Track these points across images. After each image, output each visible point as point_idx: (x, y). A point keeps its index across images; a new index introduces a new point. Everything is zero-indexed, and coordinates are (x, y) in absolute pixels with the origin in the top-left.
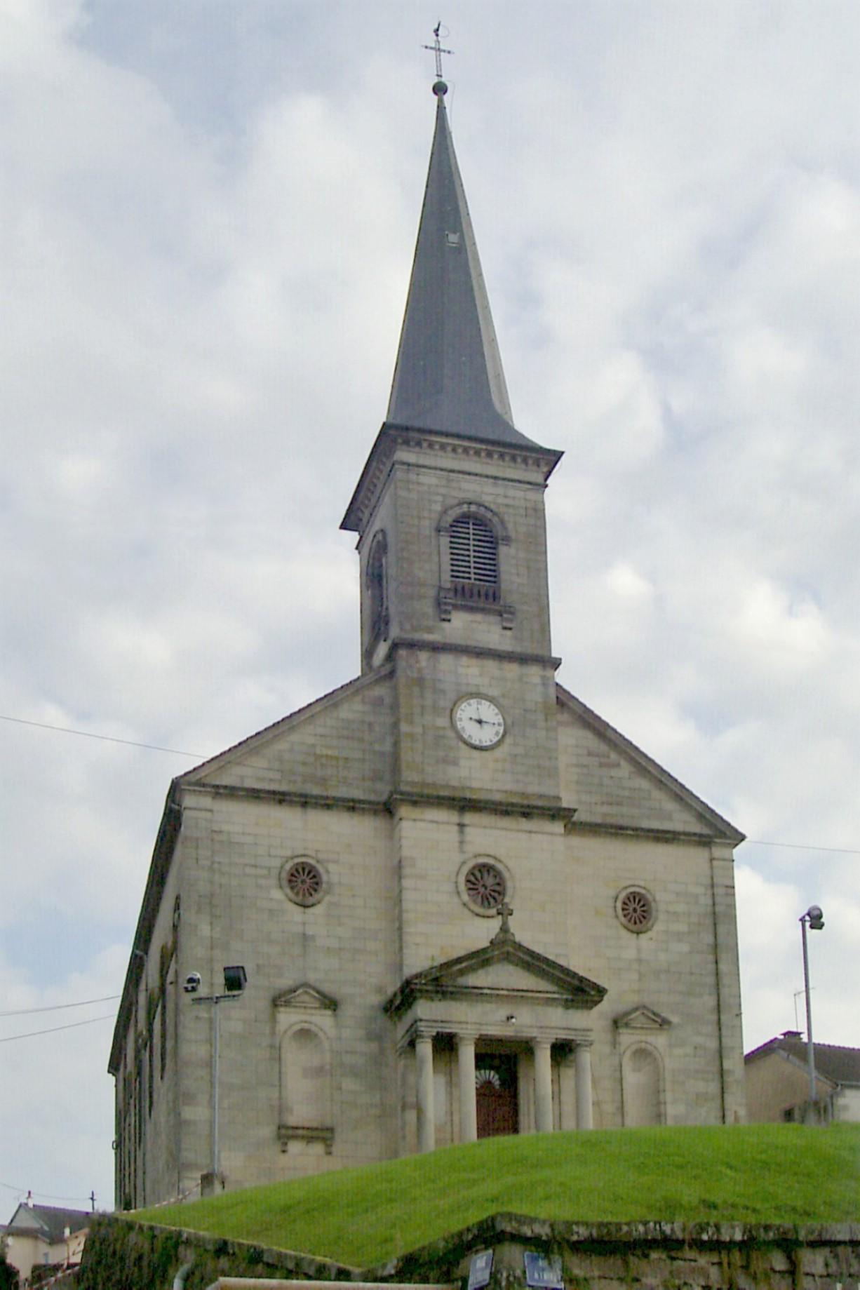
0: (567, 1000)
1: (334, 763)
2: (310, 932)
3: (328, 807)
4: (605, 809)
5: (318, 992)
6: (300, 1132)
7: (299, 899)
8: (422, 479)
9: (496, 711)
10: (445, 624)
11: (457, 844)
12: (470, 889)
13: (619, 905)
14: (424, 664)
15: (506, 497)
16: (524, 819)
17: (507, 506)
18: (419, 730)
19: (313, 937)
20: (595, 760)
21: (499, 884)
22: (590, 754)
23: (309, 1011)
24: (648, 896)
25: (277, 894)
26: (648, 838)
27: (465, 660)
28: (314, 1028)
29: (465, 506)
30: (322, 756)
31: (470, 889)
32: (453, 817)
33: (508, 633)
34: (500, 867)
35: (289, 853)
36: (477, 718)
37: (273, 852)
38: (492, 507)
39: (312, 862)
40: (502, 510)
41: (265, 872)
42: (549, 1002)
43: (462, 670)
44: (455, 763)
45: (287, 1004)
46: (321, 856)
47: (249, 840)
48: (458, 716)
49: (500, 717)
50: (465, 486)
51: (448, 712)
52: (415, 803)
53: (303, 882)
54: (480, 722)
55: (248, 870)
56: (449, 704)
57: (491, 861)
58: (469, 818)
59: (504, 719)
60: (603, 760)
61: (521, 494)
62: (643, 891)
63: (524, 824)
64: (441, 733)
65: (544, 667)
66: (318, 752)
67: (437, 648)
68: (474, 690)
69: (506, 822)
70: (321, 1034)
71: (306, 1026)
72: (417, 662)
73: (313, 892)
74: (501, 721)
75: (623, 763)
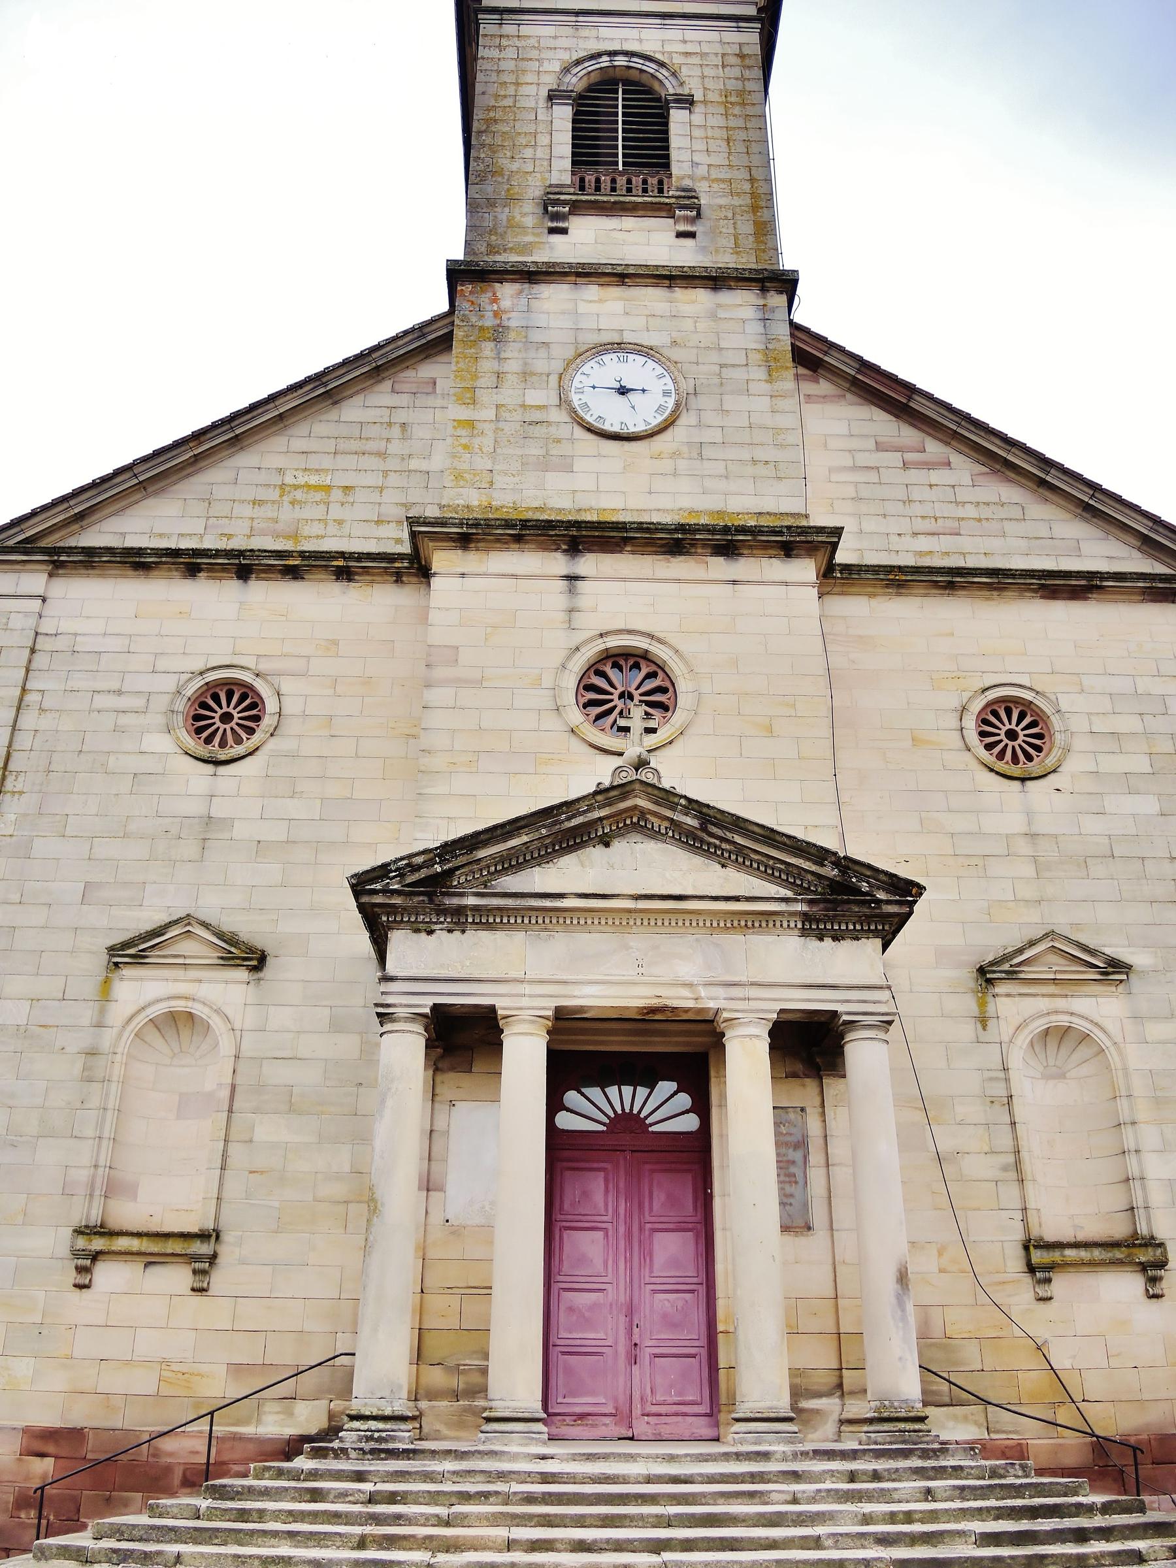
0: (806, 917)
1: (319, 496)
2: (219, 810)
3: (293, 573)
4: (924, 543)
5: (220, 935)
6: (122, 1243)
7: (202, 750)
8: (525, 30)
9: (660, 370)
10: (557, 239)
11: (562, 616)
12: (599, 717)
13: (970, 723)
14: (506, 303)
15: (685, 42)
16: (720, 560)
17: (687, 54)
18: (490, 414)
19: (227, 823)
20: (895, 458)
21: (652, 675)
22: (880, 447)
23: (193, 974)
24: (1040, 702)
25: (161, 743)
26: (1027, 588)
27: (592, 291)
28: (198, 1009)
29: (605, 58)
30: (296, 487)
31: (599, 717)
32: (558, 563)
33: (689, 242)
34: (659, 651)
35: (199, 665)
36: (630, 395)
37: (162, 664)
38: (659, 56)
39: (247, 677)
40: (677, 60)
41: (140, 703)
42: (764, 921)
43: (583, 308)
44: (568, 468)
45: (139, 959)
46: (263, 667)
47: (111, 644)
48: (576, 383)
49: (668, 380)
50: (604, 32)
51: (554, 379)
52: (464, 541)
53: (227, 718)
54: (623, 391)
55: (101, 701)
56: (558, 366)
57: (641, 643)
58: (588, 563)
59: (675, 381)
60: (909, 456)
61: (714, 36)
62: (1028, 695)
63: (719, 566)
64: (537, 416)
65: (764, 290)
66: (289, 480)
67: (532, 275)
68: (606, 338)
69: (680, 566)
70: (216, 1022)
71: (180, 1005)
72: (495, 300)
73: (244, 736)
74: (671, 386)
75: (956, 459)
